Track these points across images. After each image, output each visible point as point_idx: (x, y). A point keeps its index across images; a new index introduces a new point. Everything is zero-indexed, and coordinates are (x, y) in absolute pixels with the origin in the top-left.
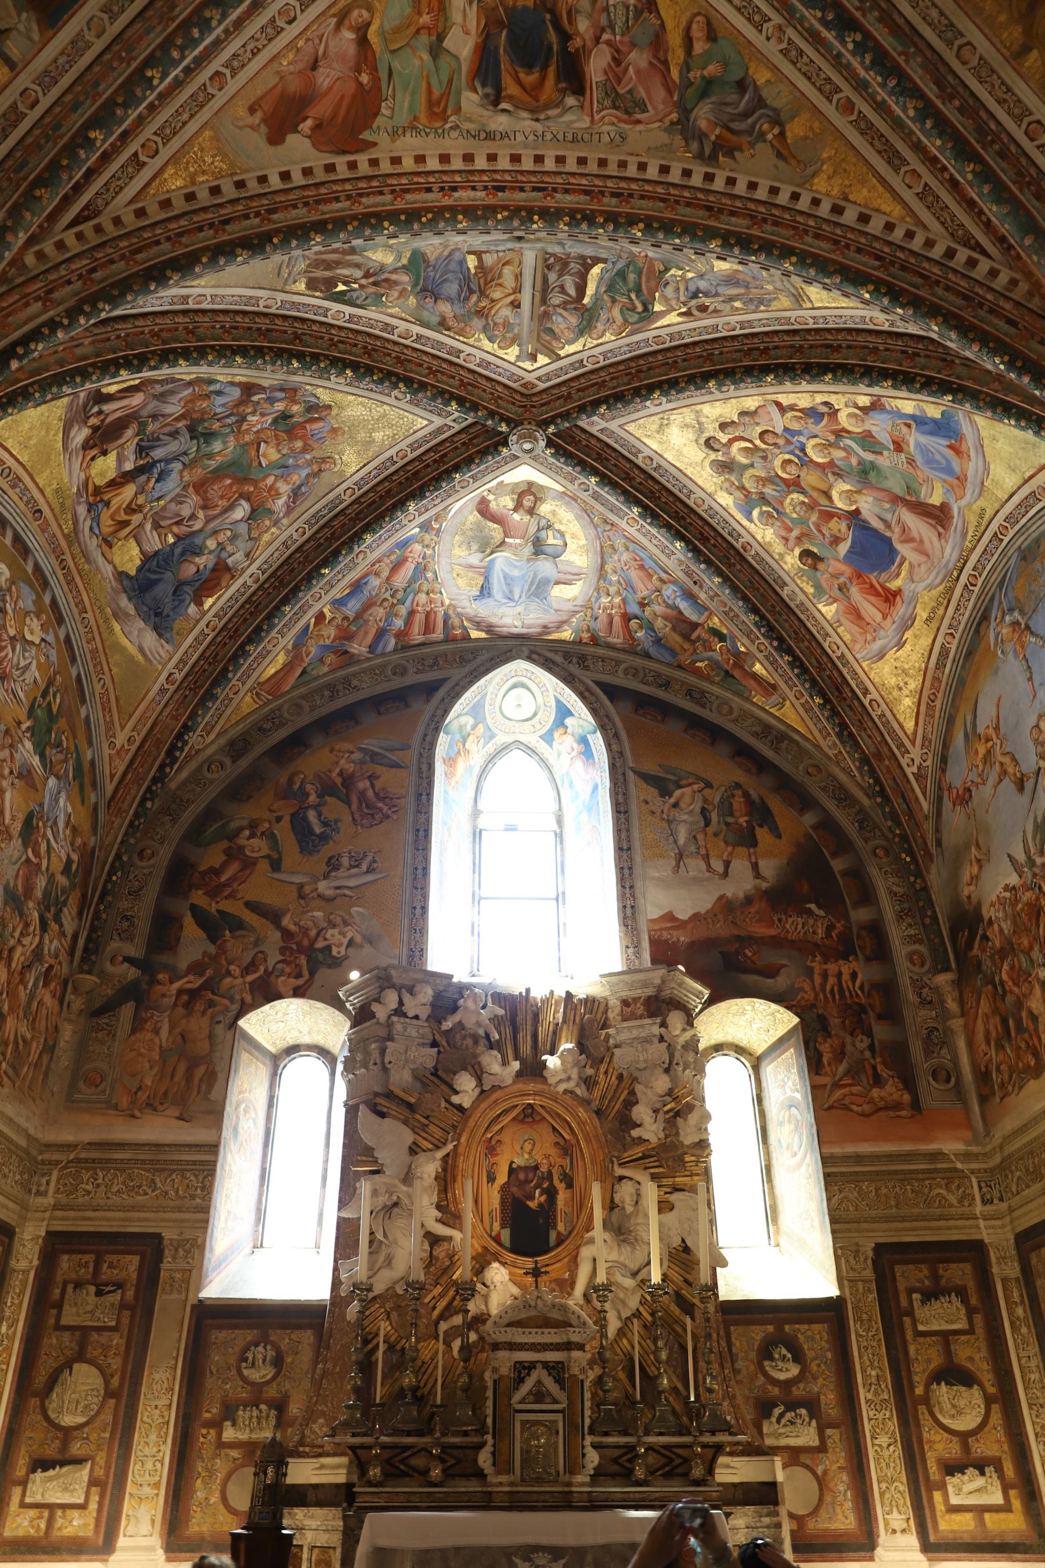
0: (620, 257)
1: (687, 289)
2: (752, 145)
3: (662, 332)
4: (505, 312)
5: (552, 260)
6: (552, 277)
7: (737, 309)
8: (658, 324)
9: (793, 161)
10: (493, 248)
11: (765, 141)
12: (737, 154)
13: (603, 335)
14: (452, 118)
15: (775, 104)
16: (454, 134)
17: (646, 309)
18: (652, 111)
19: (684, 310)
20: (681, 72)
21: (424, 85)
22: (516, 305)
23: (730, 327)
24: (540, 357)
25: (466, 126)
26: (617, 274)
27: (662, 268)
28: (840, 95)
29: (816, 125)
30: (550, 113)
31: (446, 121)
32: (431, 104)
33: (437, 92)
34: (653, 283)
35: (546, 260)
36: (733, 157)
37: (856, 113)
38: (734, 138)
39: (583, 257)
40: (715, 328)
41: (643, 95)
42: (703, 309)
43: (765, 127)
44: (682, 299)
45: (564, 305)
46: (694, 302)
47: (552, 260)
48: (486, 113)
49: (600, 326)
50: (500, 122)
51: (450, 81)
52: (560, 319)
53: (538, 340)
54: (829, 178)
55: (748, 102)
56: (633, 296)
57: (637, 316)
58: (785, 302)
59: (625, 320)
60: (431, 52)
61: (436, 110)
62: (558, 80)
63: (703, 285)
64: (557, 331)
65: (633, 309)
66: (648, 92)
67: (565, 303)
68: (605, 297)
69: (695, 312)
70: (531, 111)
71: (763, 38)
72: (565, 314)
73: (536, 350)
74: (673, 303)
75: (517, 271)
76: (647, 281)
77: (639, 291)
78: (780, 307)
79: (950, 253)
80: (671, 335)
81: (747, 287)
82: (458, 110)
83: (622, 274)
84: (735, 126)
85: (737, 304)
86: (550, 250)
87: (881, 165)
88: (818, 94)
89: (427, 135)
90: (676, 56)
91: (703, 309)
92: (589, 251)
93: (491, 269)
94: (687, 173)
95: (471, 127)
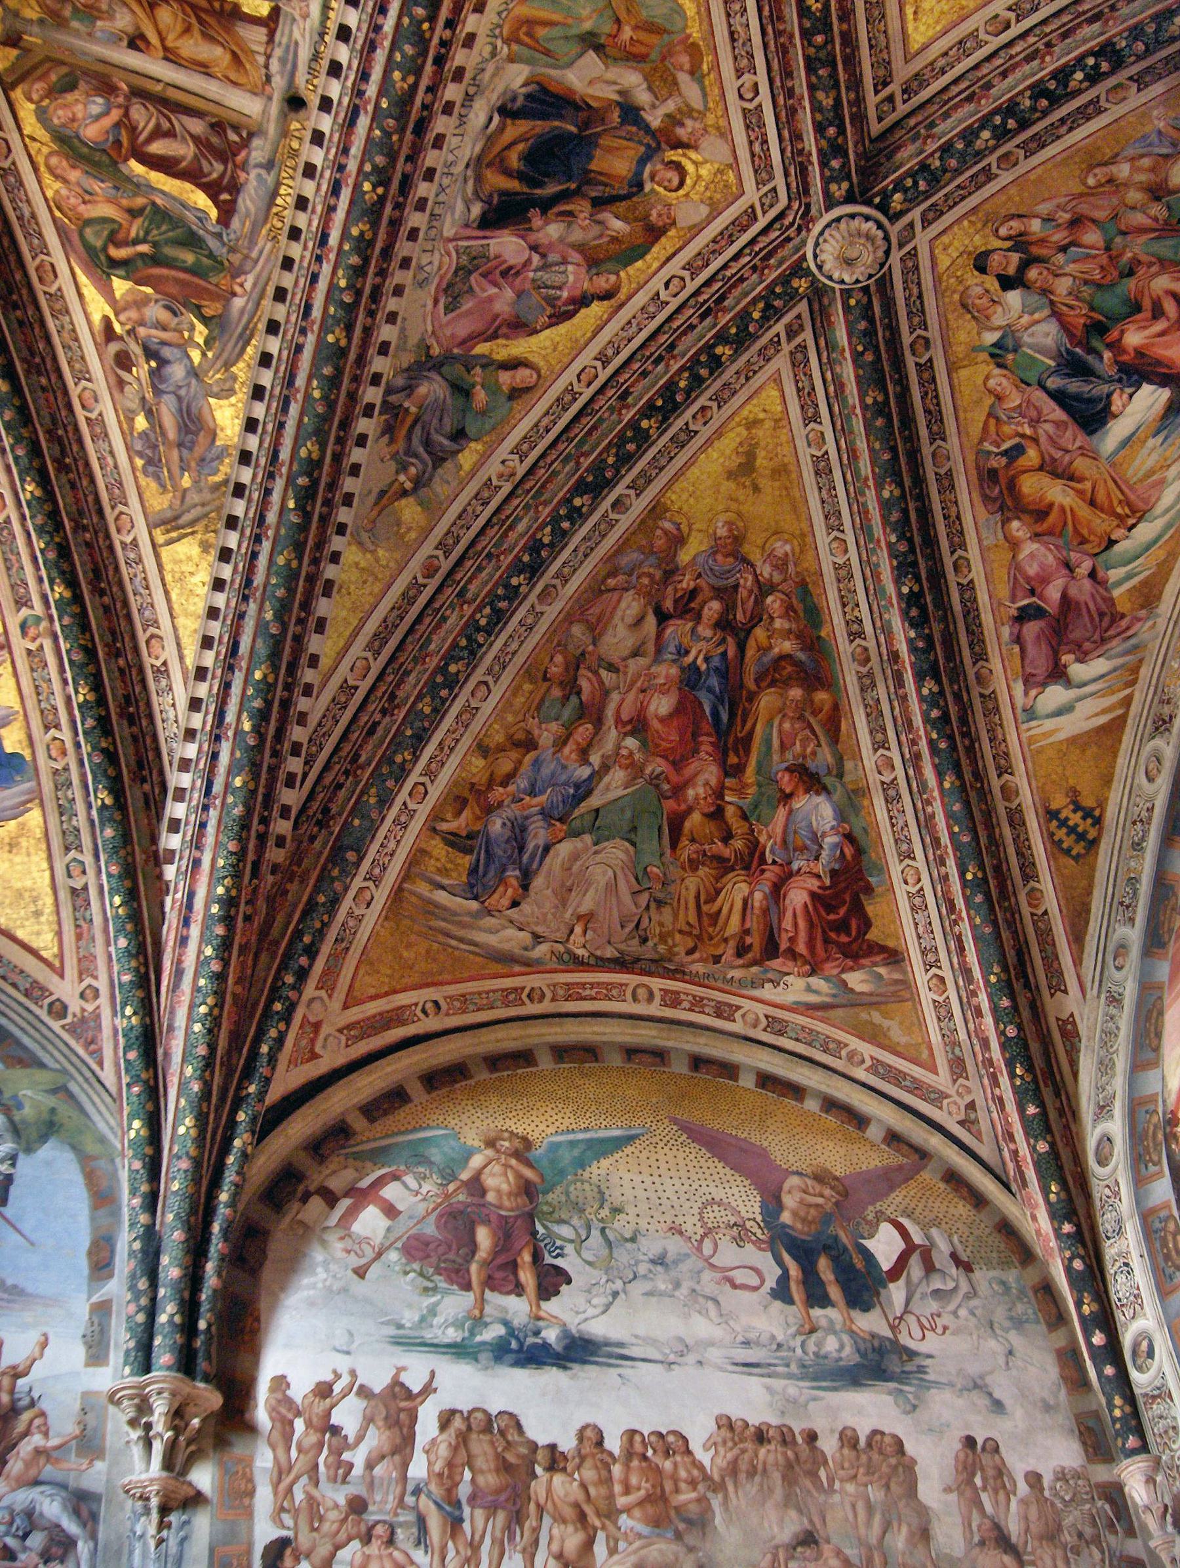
0: (232, 250)
1: (164, 343)
2: (394, 456)
3: (64, 280)
4: (123, 21)
5: (233, 137)
6: (197, 126)
7: (131, 421)
8: (83, 279)
9: (375, 513)
10: (278, 52)
11: (397, 473)
12: (386, 439)
13: (57, 177)
14: (506, 49)
15: (437, 479)
16: (489, 48)
17: (114, 263)
18: (445, 320)
19: (118, 328)
20: (483, 356)
21: (555, 17)
22: (136, 42)
23: (90, 402)
24: (14, 53)
25: (490, 68)
26: (193, 234)
27: (208, 312)
28: (442, 558)
29: (413, 535)
30: (471, 183)
31: (507, 41)
32: (531, 23)
33: (541, 32)
34: (174, 290)
35: (236, 128)
36: (383, 434)
37: (425, 581)
38: (404, 432)
39: (235, 188)
40: (83, 375)
41: (465, 308)
42: (123, 361)
43: (413, 470)
44: (142, 331)
45: (126, 124)
46: (135, 349)
47: (233, 137)
48: (495, 96)
49: (74, 175)
50: (479, 114)
51: (547, 53)
52: (95, 109)
53: (48, 59)
54: (357, 564)
55: (441, 445)
56: (144, 248)
57: (99, 244)
58: (160, 502)
59: (89, 222)
60: (592, 33)
61: (524, 29)
62: (503, 193)
63: (177, 372)
64: (70, 97)
65: (114, 239)
66: (469, 312)
67: (133, 130)
68: (140, 201)
69: (114, 347)
70: (479, 159)
71: (505, 457)
72: (107, 122)
73: (27, 51)
74: (133, 314)
75: (215, 70)
76: (177, 281)
77: (155, 260)
78: (147, 495)
79: (296, 750)
80: (59, 296)
81: (180, 445)
82: (511, 59)
83: (192, 241)
84: (418, 431)
85: (141, 423)
86: (256, 142)
87: (372, 626)
88: (445, 530)
89: (499, 14)
90: (502, 350)
91: (123, 361)
92: (248, 202)
93: (228, 30)
94: (376, 379)
95: (487, 75)
